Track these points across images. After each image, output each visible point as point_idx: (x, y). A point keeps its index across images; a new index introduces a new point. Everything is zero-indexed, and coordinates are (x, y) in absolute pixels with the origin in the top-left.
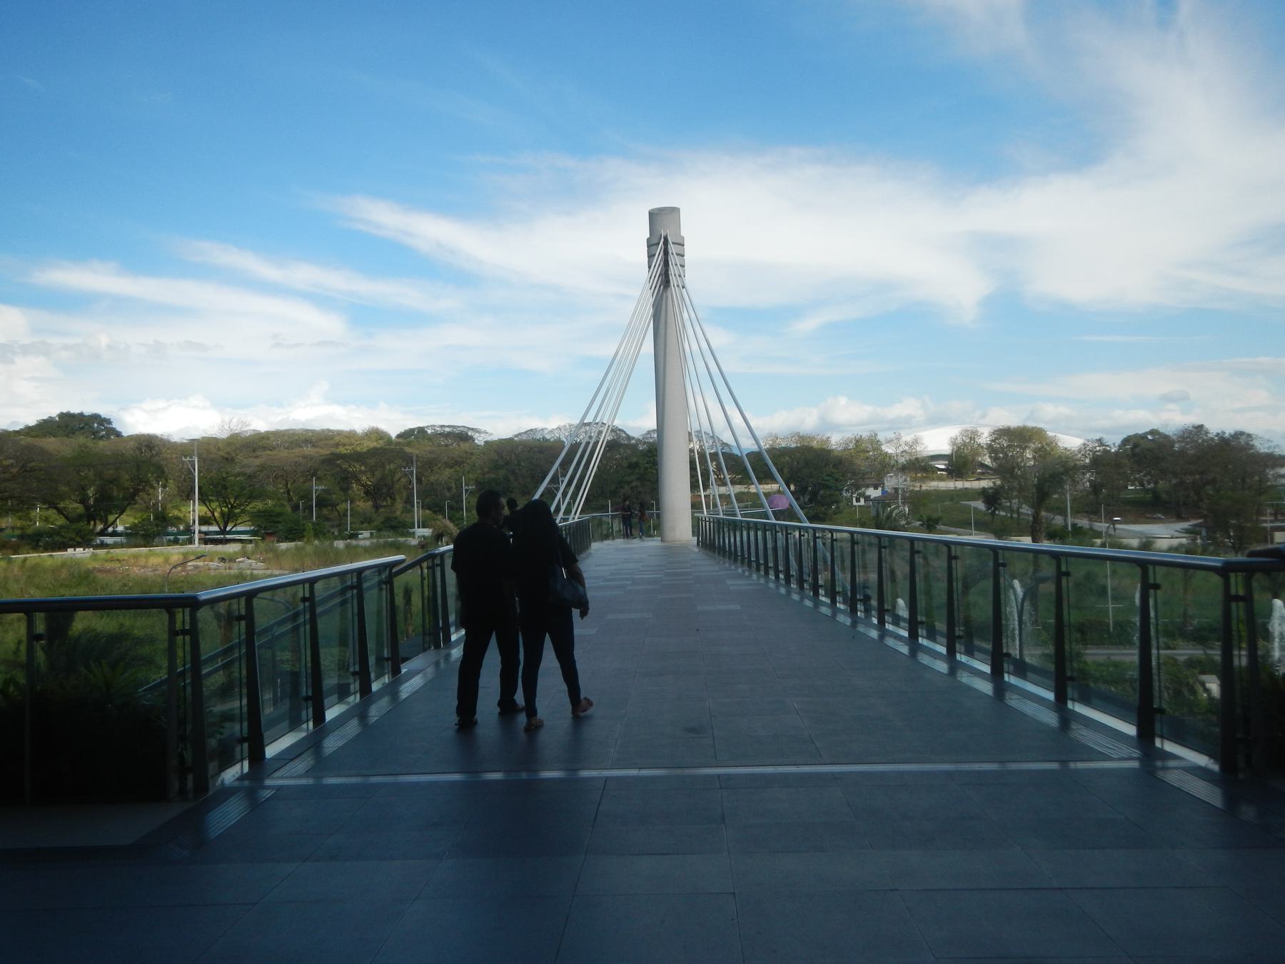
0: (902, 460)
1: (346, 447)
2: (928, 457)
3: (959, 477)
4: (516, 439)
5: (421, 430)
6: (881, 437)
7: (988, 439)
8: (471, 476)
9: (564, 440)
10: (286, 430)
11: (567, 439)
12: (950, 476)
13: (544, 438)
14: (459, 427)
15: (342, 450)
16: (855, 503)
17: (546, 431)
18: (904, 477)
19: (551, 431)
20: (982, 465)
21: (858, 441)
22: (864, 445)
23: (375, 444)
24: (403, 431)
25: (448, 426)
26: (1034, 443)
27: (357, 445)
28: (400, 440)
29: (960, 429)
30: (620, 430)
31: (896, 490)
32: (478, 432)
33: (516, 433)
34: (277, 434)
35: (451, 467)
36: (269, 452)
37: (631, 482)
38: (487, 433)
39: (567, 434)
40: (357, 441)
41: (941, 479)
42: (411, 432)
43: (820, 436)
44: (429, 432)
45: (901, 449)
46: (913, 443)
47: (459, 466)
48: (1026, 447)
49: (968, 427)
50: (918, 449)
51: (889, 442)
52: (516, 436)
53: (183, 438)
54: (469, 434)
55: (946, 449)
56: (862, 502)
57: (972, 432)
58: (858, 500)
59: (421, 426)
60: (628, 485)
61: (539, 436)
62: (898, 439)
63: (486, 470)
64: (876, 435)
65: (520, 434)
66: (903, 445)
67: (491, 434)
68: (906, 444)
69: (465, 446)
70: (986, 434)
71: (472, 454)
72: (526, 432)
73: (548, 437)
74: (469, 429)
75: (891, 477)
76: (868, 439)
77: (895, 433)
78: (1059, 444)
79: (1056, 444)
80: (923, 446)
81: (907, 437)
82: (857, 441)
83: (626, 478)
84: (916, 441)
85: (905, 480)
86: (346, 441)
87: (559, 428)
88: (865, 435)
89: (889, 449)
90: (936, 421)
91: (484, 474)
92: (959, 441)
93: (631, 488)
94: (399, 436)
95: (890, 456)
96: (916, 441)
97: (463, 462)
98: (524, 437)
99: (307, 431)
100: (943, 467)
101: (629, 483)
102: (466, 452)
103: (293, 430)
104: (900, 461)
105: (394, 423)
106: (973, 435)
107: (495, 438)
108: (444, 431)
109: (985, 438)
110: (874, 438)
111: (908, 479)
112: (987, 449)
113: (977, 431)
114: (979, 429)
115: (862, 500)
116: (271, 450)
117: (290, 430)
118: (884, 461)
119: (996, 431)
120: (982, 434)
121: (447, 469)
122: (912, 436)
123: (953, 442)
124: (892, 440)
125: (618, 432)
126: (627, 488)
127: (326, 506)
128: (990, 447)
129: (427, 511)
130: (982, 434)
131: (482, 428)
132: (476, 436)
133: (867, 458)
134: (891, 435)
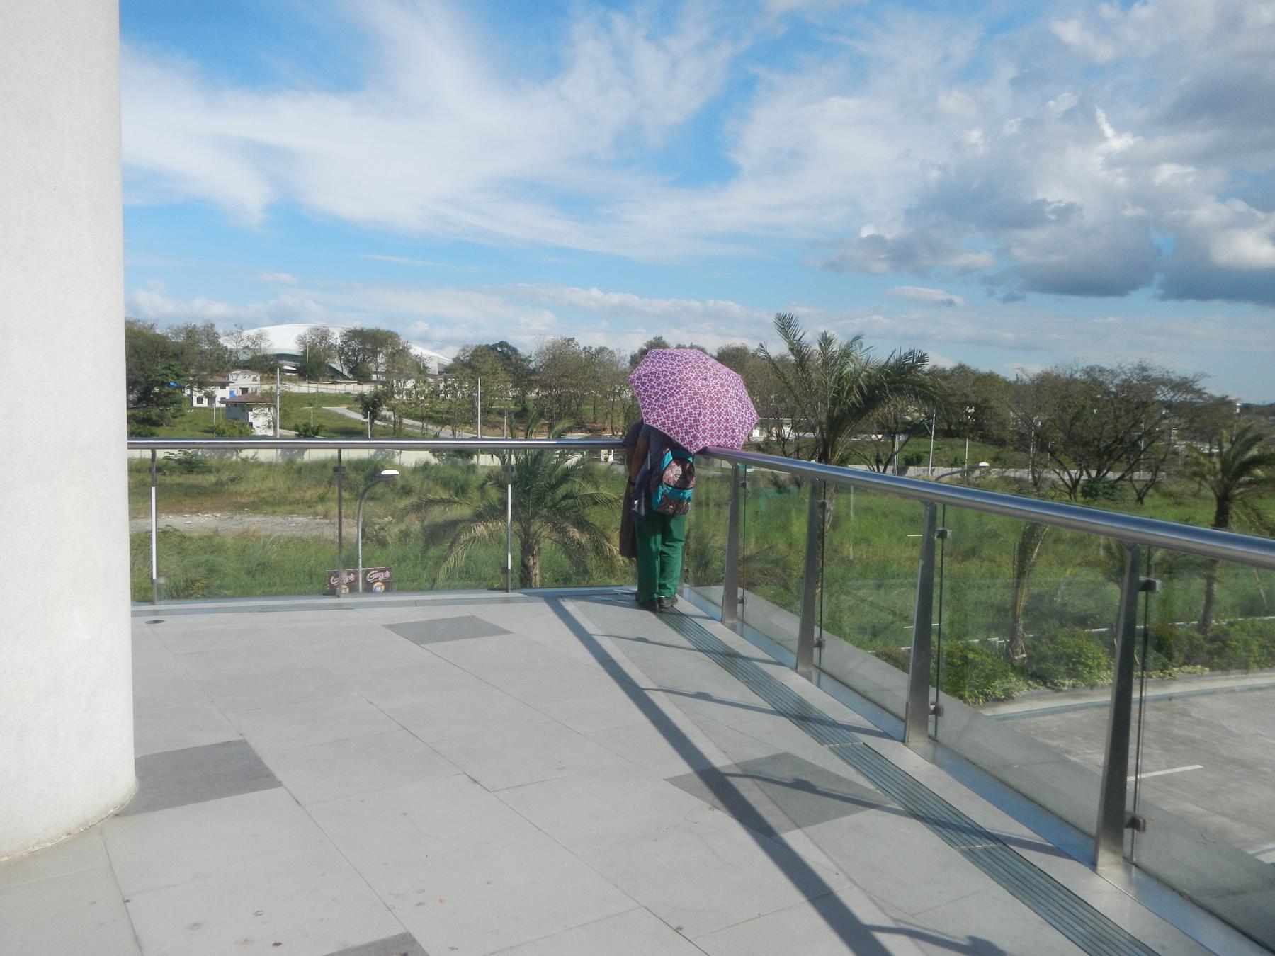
0: (243, 357)
2: (273, 355)
3: (312, 379)
6: (219, 329)
7: (339, 341)
12: (302, 378)
16: (195, 404)
18: (252, 377)
20: (336, 371)
21: (191, 333)
22: (197, 337)
26: (387, 348)
29: (307, 328)
31: (244, 390)
41: (290, 380)
43: (141, 323)
45: (242, 345)
46: (257, 338)
48: (379, 352)
49: (317, 324)
50: (263, 345)
51: (228, 335)
55: (292, 348)
56: (205, 403)
57: (322, 331)
58: (200, 400)
62: (240, 333)
64: (213, 326)
66: (245, 340)
68: (249, 338)
70: (337, 335)
75: (238, 375)
76: (204, 330)
77: (236, 325)
78: (411, 351)
79: (408, 349)
80: (268, 343)
81: (252, 332)
82: (190, 331)
84: (260, 337)
85: (255, 379)
88: (200, 324)
89: (228, 343)
90: (282, 317)
92: (308, 339)
95: (231, 352)
96: (260, 337)
100: (295, 369)
104: (241, 359)
106: (324, 336)
109: (336, 339)
110: (210, 330)
111: (258, 378)
112: (338, 351)
113: (327, 330)
114: (330, 329)
115: (205, 400)
118: (223, 357)
119: (349, 332)
120: (334, 334)
122: (256, 330)
123: (302, 341)
124: (233, 334)
128: (342, 349)
130: (334, 334)
133: (202, 352)
134: (234, 329)
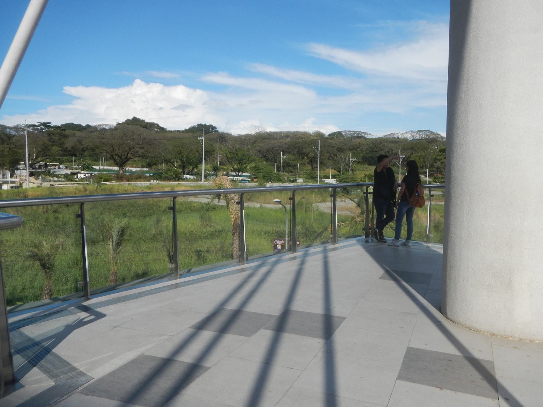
1: (302, 139)
4: (384, 137)
5: (340, 133)
8: (360, 155)
9: (408, 138)
10: (280, 132)
11: (410, 138)
13: (398, 138)
14: (358, 131)
15: (300, 140)
17: (399, 134)
19: (403, 134)
23: (316, 138)
24: (331, 133)
25: (352, 131)
27: (308, 138)
28: (329, 137)
30: (438, 134)
32: (366, 134)
33: (384, 135)
34: (275, 133)
35: (352, 150)
36: (269, 141)
37: (441, 159)
38: (371, 135)
39: (410, 136)
40: (307, 136)
42: (334, 134)
44: (344, 133)
47: (356, 150)
52: (385, 136)
53: (235, 134)
54: (362, 135)
59: (339, 130)
60: (439, 161)
61: (396, 136)
63: (368, 152)
65: (386, 135)
67: (373, 135)
69: (359, 140)
71: (362, 144)
72: (389, 135)
73: (400, 137)
74: (362, 133)
83: (440, 158)
86: (303, 136)
87: (406, 133)
91: (367, 154)
93: (442, 163)
94: (329, 135)
97: (358, 148)
98: (388, 137)
99: (289, 132)
101: (439, 160)
102: (360, 143)
103: (283, 131)
105: (327, 130)
107: (374, 137)
108: (350, 134)
116: (270, 140)
117: (282, 132)
121: (349, 151)
125: (437, 135)
126: (439, 163)
127: (290, 166)
129: (336, 171)
131: (368, 132)
132: (366, 136)
